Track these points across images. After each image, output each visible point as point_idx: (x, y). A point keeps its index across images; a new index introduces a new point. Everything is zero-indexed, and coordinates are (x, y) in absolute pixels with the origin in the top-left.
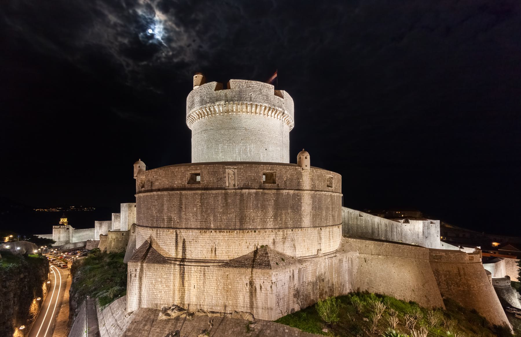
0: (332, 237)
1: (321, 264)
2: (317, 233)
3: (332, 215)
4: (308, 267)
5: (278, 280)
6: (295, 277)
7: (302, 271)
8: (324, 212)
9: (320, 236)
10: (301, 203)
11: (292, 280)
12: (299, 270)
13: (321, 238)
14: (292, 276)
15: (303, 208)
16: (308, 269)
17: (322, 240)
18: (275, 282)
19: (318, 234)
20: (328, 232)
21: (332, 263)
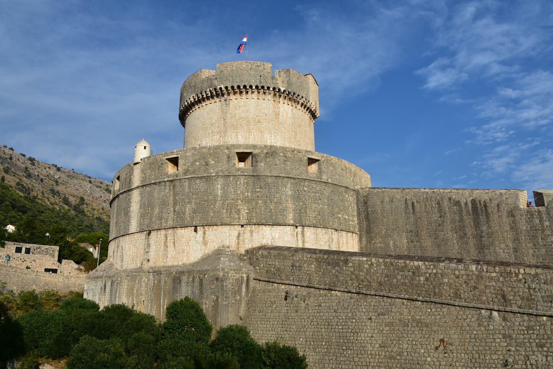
0: (171, 243)
1: (141, 280)
2: (144, 237)
3: (174, 211)
4: (123, 281)
5: (90, 288)
6: (106, 290)
7: (115, 284)
8: (156, 211)
9: (148, 241)
10: (131, 203)
11: (103, 292)
12: (112, 282)
13: (149, 245)
14: (103, 287)
15: (132, 208)
16: (123, 283)
17: (151, 247)
18: (86, 290)
19: (146, 239)
20: (162, 236)
21: (159, 281)
